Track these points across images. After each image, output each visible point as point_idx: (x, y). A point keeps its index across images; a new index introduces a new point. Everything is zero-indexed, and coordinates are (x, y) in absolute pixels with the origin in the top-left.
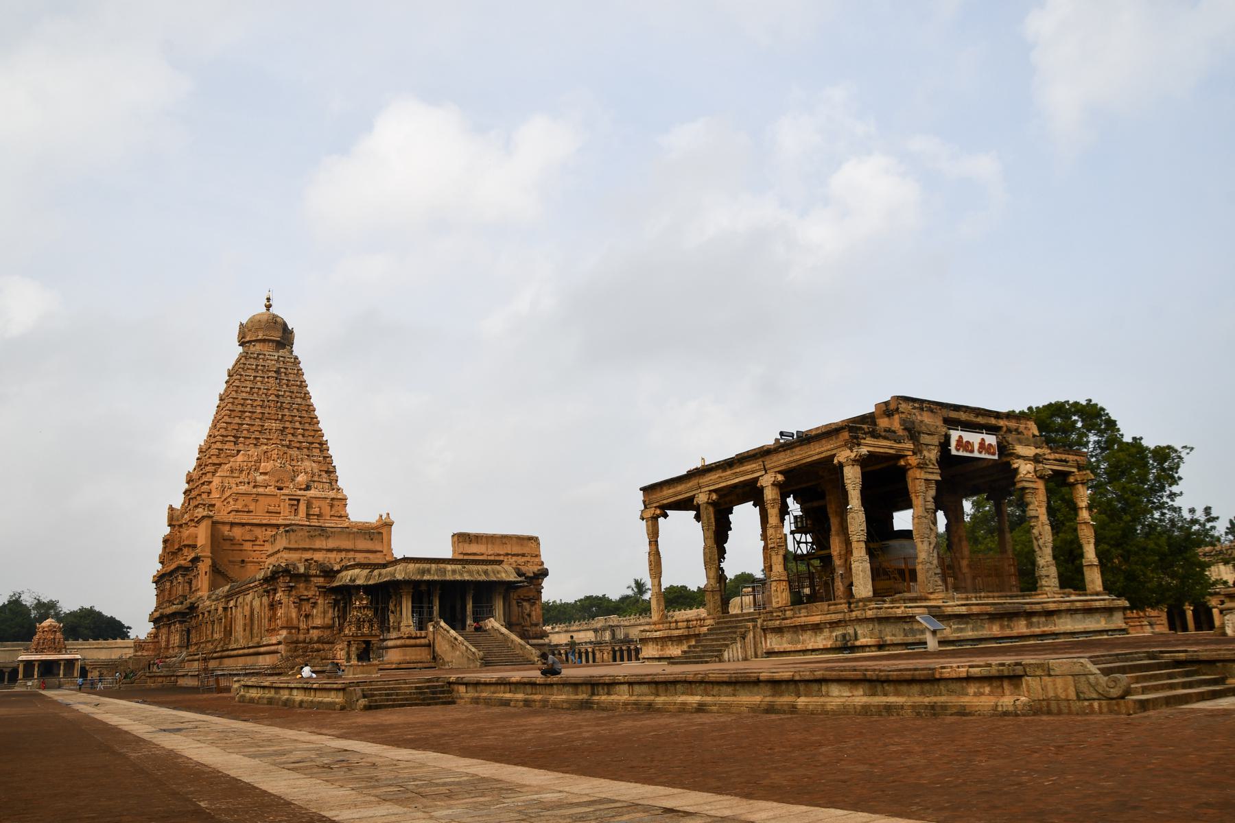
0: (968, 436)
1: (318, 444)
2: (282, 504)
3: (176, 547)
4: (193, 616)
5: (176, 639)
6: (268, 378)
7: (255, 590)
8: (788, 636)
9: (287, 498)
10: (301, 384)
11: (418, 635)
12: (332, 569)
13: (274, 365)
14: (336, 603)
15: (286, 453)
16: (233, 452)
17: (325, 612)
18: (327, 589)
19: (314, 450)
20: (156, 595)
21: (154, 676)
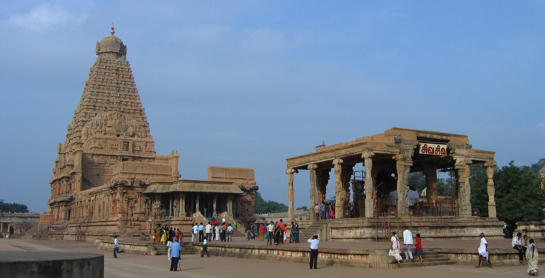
0: (429, 145)
1: (140, 110)
4: (72, 203)
5: (62, 215)
6: (112, 73)
8: (340, 231)
10: (130, 77)
11: (188, 219)
12: (145, 184)
13: (116, 66)
14: (147, 201)
15: (121, 116)
16: (93, 114)
17: (141, 206)
19: (137, 114)
20: (52, 190)
21: (52, 234)
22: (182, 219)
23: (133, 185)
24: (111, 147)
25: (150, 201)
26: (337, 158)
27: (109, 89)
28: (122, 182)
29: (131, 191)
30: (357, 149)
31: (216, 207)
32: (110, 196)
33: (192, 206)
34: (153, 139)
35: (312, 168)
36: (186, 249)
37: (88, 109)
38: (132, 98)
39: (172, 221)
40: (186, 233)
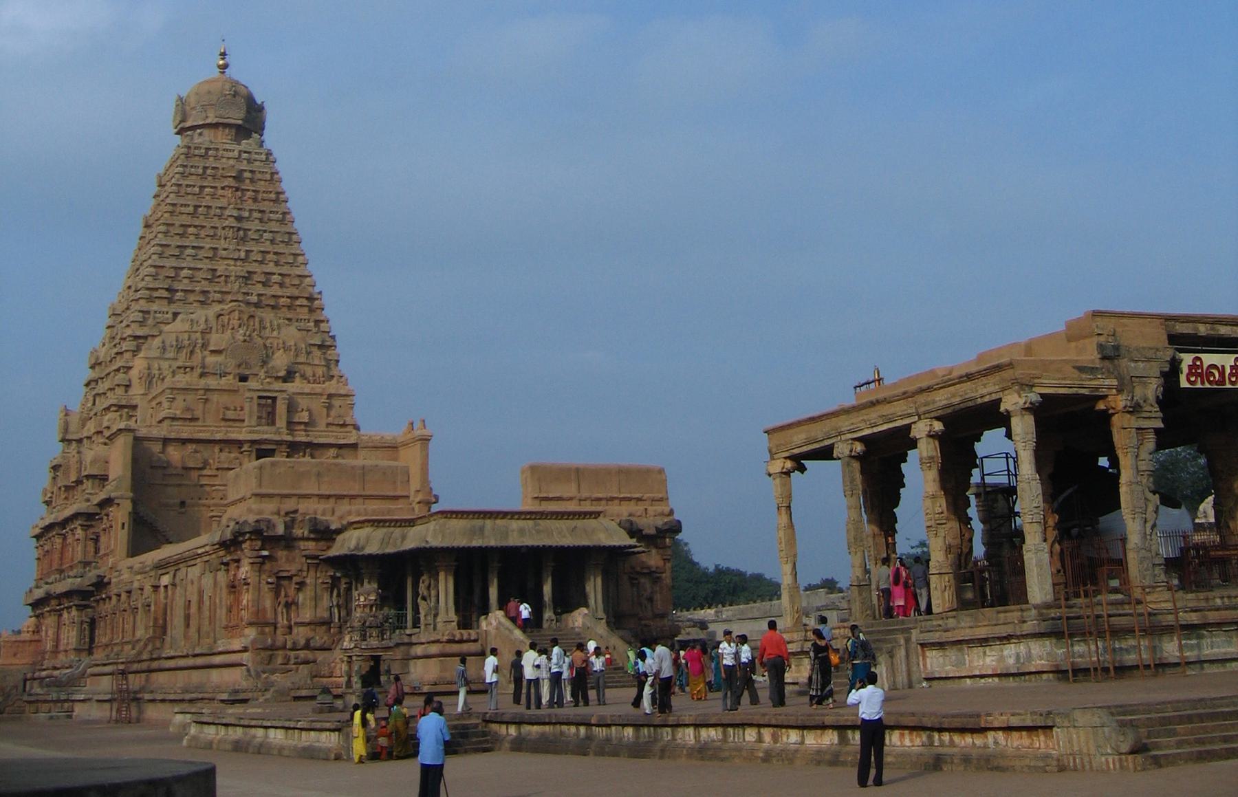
2: (247, 406)
7: (206, 559)
12: (329, 527)
14: (335, 582)
15: (252, 316)
17: (316, 599)
18: (321, 560)
22: (446, 638)
23: (291, 532)
24: (221, 417)
25: (346, 583)
26: (922, 417)
28: (257, 524)
29: (285, 553)
30: (985, 385)
31: (550, 595)
32: (220, 569)
33: (477, 591)
35: (848, 453)
39: (416, 644)
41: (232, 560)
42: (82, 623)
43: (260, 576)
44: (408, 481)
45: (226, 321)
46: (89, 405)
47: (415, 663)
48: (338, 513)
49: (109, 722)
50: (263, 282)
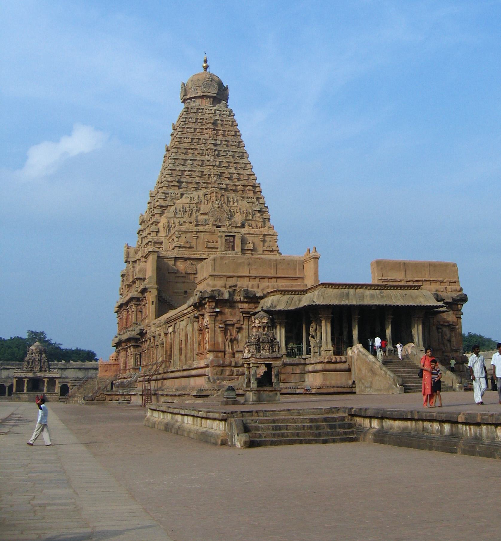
1: (252, 186)
2: (219, 240)
3: (131, 281)
6: (206, 129)
7: (188, 316)
9: (224, 234)
10: (236, 135)
11: (338, 360)
13: (212, 118)
22: (326, 360)
23: (233, 298)
24: (206, 246)
27: (202, 154)
28: (212, 293)
29: (230, 310)
31: (390, 335)
33: (345, 333)
34: (275, 230)
36: (332, 427)
37: (168, 187)
38: (239, 166)
40: (336, 387)
41: (200, 315)
42: (136, 355)
43: (215, 324)
44: (303, 269)
45: (209, 197)
46: (139, 243)
47: (308, 376)
48: (261, 288)
49: (141, 406)
50: (228, 178)
